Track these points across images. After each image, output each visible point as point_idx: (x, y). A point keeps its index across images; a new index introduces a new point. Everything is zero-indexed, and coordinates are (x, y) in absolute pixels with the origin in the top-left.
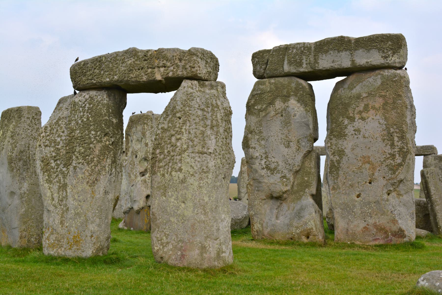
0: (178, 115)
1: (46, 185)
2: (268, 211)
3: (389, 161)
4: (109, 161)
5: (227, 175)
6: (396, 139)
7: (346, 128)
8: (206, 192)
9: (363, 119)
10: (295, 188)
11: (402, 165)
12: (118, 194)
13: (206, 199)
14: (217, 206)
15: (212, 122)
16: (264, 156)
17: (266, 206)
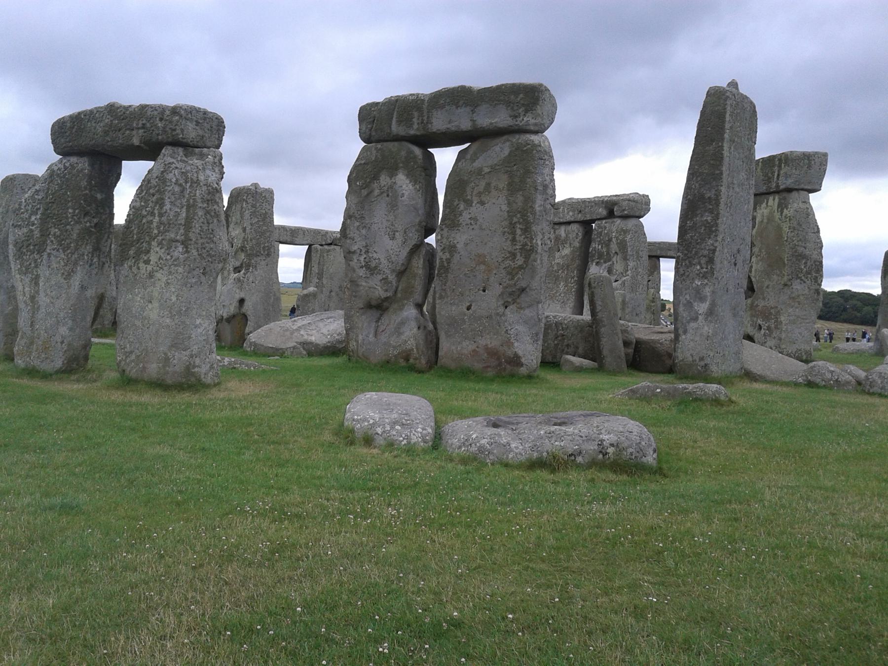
0: (151, 191)
1: (18, 276)
2: (365, 324)
3: (508, 262)
4: (89, 248)
5: (208, 269)
6: (519, 232)
7: (461, 215)
8: (173, 290)
9: (482, 203)
10: (399, 295)
11: (524, 269)
12: (103, 290)
13: (174, 298)
14: (188, 308)
15: (188, 201)
16: (364, 251)
17: (364, 317)
